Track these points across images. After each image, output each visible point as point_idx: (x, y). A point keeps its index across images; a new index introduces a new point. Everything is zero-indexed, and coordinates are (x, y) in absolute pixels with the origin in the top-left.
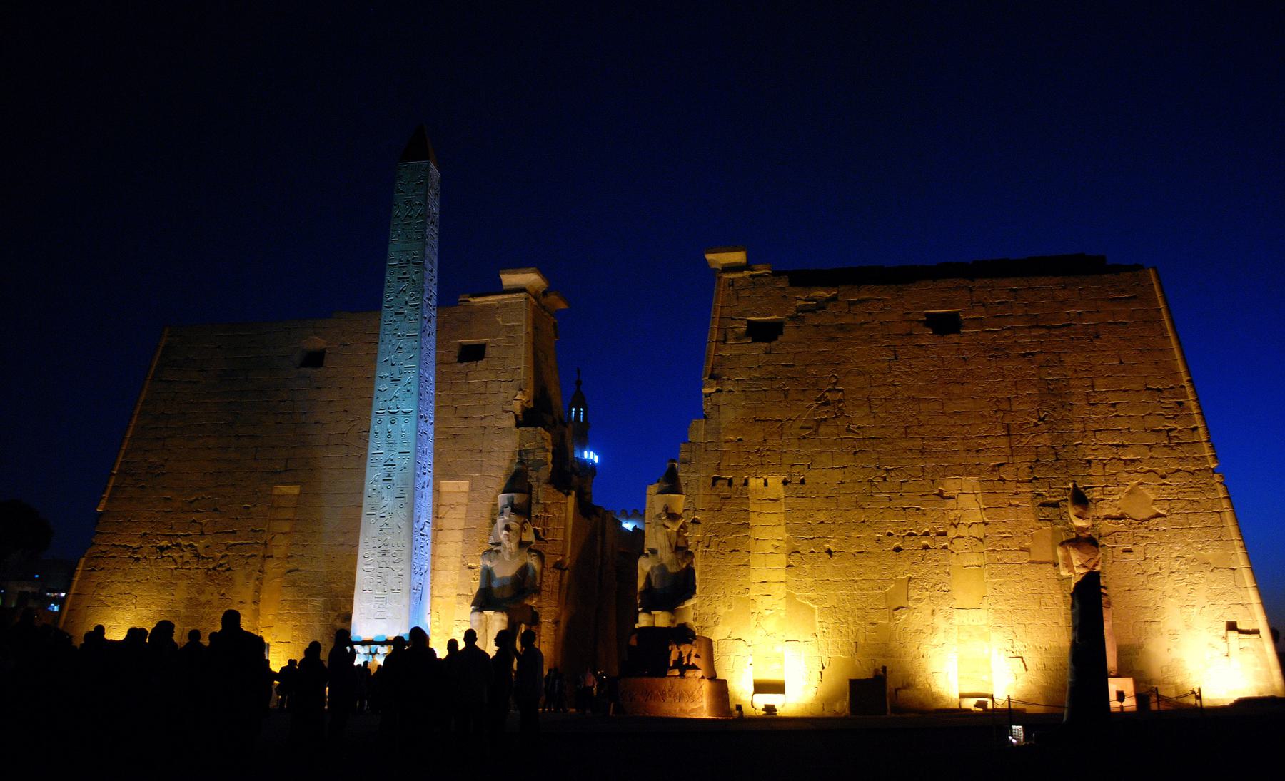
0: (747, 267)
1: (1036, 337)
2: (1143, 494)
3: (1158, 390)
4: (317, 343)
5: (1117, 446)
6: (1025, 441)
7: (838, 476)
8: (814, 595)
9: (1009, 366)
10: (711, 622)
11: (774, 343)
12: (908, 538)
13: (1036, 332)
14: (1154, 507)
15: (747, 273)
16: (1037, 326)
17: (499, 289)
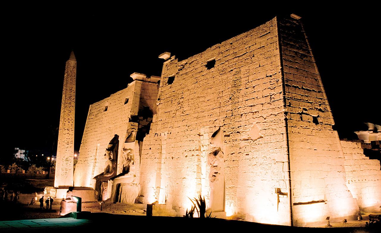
0: (170, 58)
1: (234, 62)
2: (257, 128)
3: (271, 76)
4: (107, 104)
5: (251, 106)
6: (224, 109)
7: (177, 130)
8: (167, 173)
9: (224, 77)
10: (149, 182)
11: (172, 84)
12: (189, 152)
13: (235, 60)
14: (260, 133)
15: (170, 60)
16: (236, 57)
17: (131, 80)
